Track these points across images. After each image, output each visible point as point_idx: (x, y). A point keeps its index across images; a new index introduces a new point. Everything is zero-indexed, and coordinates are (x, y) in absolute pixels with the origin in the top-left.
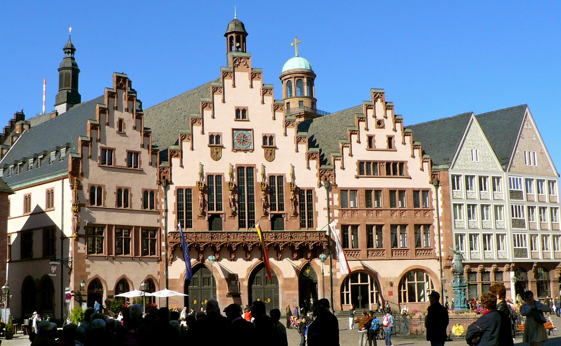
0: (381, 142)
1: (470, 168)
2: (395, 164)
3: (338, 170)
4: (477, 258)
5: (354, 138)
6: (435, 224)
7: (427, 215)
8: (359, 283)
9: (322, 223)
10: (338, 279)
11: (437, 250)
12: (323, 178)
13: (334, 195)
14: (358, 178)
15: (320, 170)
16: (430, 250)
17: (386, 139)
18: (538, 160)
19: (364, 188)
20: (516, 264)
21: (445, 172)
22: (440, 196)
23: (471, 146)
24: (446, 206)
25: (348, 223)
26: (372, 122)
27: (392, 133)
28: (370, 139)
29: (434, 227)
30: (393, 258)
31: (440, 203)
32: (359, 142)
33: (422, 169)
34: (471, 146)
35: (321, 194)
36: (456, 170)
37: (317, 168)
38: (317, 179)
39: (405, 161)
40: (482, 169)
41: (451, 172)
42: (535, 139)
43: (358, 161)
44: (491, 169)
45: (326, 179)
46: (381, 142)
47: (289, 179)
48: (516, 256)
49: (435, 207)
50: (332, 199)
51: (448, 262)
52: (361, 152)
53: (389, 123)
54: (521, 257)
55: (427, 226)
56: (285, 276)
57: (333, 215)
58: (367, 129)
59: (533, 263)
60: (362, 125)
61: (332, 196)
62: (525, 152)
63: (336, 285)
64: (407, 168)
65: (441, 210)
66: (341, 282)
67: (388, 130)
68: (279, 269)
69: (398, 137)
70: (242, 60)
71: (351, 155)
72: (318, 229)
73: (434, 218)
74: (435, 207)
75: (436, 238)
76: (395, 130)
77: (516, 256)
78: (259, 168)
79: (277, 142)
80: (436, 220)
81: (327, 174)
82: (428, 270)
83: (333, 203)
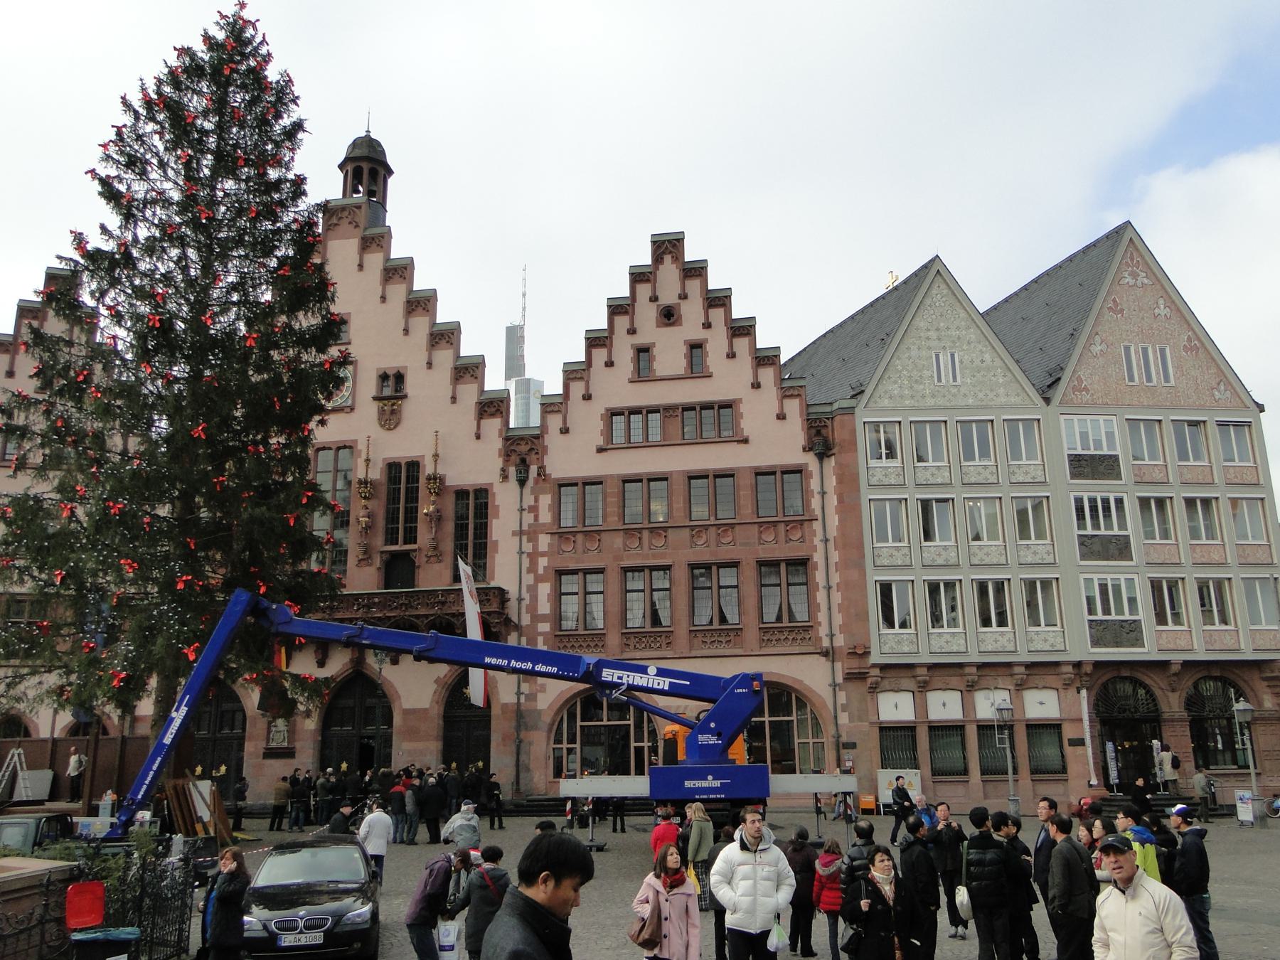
0: (670, 357)
1: (930, 402)
2: (707, 406)
3: (553, 440)
4: (955, 649)
5: (600, 355)
6: (818, 558)
7: (797, 535)
8: (605, 722)
9: (506, 570)
10: (539, 712)
11: (823, 631)
12: (514, 458)
13: (542, 497)
14: (601, 450)
15: (507, 439)
16: (807, 629)
17: (684, 349)
18: (1178, 368)
19: (618, 476)
20: (1098, 665)
21: (846, 417)
22: (831, 482)
23: (934, 343)
24: (849, 506)
25: (572, 566)
26: (647, 314)
27: (698, 334)
28: (643, 351)
29: (815, 567)
30: (694, 653)
31: (832, 500)
32: (610, 364)
33: (781, 417)
34: (934, 343)
35: (506, 499)
36: (884, 410)
37: (500, 435)
38: (499, 463)
39: (734, 401)
40: (970, 401)
41: (863, 416)
42: (1162, 311)
43: (607, 410)
44: (1003, 400)
45: (523, 461)
46: (670, 357)
47: (428, 469)
48: (1096, 642)
49: (818, 512)
50: (534, 509)
51: (854, 664)
52: (616, 387)
53: (692, 311)
54: (1118, 645)
55: (801, 564)
56: (406, 705)
57: (535, 547)
58: (632, 331)
59: (1164, 665)
60: (622, 322)
61: (536, 500)
62: (1127, 349)
63: (535, 727)
64: (741, 415)
65: (833, 521)
66: (547, 719)
67: (691, 326)
68: (392, 686)
69: (717, 341)
70: (346, 213)
71: (587, 397)
72: (493, 584)
73: (817, 541)
74: (818, 512)
75: (821, 596)
76: (707, 325)
77: (1096, 642)
78: (361, 446)
79: (410, 387)
80: (820, 546)
81: (523, 448)
82: (796, 686)
83: (536, 518)
